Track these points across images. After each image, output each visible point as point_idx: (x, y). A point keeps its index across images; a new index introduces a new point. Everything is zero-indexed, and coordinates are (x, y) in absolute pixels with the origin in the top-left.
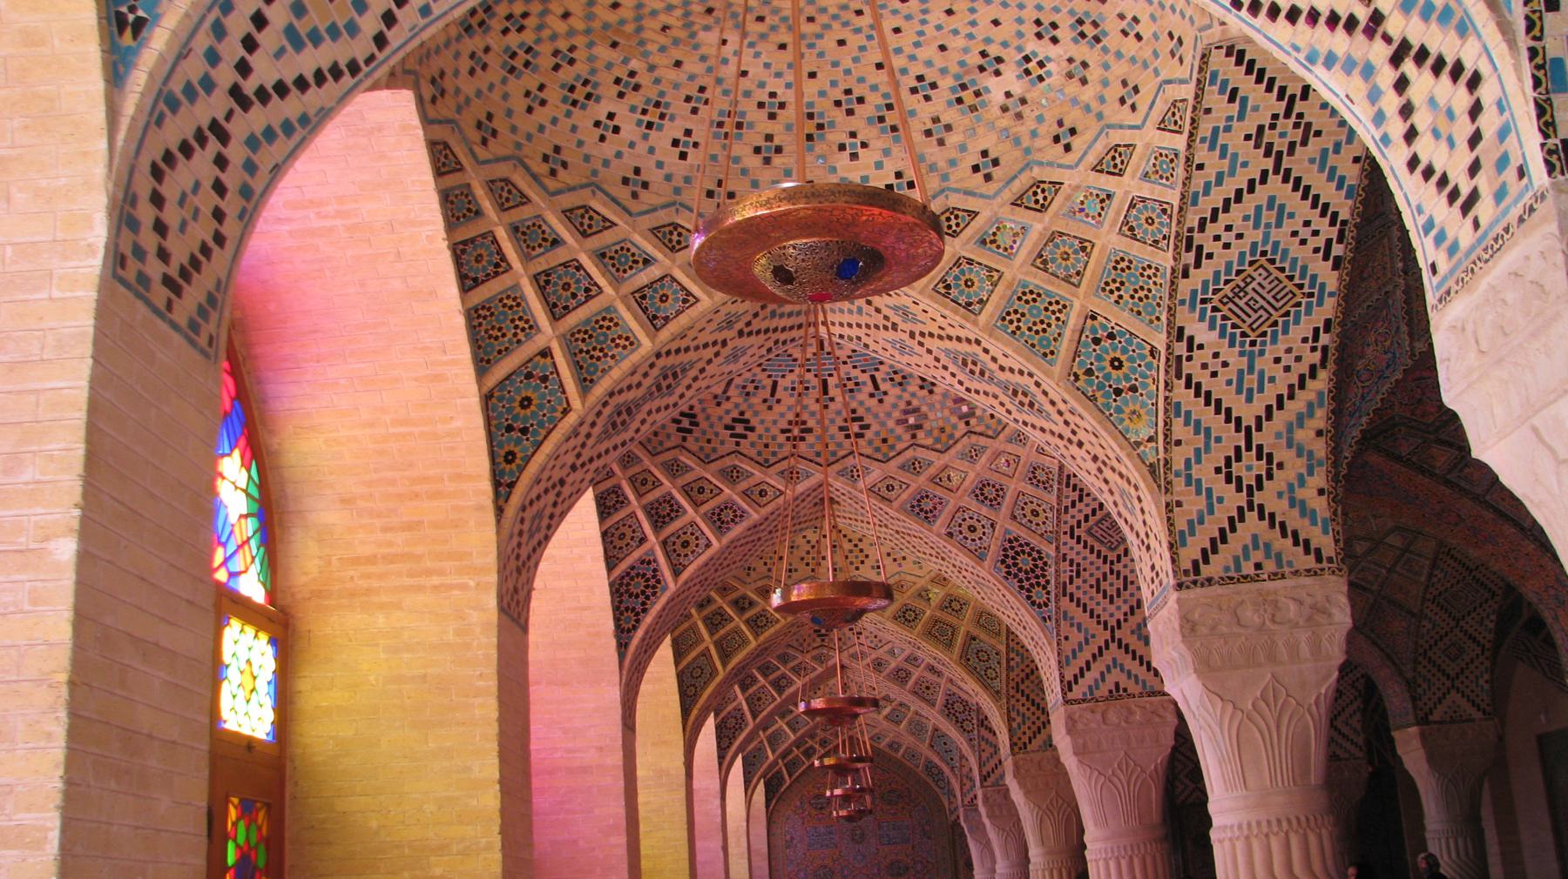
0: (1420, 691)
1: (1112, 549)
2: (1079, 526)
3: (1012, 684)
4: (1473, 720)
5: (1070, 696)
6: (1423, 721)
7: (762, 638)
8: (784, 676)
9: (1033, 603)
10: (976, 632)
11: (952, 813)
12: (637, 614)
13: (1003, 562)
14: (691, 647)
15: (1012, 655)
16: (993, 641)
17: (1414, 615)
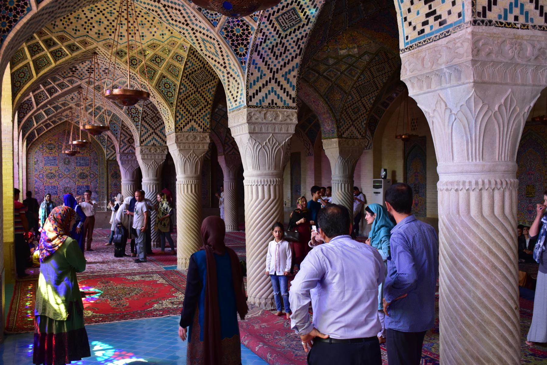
0: (341, 124)
1: (284, 31)
2: (273, 15)
3: (179, 100)
4: (358, 139)
5: (250, 103)
6: (340, 137)
7: (58, 63)
8: (53, 88)
9: (237, 54)
10: (165, 74)
11: (107, 155)
12: (10, 22)
13: (226, 29)
14: (20, 61)
15: (182, 87)
16: (173, 80)
17: (346, 93)
